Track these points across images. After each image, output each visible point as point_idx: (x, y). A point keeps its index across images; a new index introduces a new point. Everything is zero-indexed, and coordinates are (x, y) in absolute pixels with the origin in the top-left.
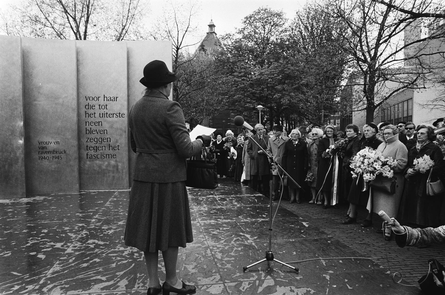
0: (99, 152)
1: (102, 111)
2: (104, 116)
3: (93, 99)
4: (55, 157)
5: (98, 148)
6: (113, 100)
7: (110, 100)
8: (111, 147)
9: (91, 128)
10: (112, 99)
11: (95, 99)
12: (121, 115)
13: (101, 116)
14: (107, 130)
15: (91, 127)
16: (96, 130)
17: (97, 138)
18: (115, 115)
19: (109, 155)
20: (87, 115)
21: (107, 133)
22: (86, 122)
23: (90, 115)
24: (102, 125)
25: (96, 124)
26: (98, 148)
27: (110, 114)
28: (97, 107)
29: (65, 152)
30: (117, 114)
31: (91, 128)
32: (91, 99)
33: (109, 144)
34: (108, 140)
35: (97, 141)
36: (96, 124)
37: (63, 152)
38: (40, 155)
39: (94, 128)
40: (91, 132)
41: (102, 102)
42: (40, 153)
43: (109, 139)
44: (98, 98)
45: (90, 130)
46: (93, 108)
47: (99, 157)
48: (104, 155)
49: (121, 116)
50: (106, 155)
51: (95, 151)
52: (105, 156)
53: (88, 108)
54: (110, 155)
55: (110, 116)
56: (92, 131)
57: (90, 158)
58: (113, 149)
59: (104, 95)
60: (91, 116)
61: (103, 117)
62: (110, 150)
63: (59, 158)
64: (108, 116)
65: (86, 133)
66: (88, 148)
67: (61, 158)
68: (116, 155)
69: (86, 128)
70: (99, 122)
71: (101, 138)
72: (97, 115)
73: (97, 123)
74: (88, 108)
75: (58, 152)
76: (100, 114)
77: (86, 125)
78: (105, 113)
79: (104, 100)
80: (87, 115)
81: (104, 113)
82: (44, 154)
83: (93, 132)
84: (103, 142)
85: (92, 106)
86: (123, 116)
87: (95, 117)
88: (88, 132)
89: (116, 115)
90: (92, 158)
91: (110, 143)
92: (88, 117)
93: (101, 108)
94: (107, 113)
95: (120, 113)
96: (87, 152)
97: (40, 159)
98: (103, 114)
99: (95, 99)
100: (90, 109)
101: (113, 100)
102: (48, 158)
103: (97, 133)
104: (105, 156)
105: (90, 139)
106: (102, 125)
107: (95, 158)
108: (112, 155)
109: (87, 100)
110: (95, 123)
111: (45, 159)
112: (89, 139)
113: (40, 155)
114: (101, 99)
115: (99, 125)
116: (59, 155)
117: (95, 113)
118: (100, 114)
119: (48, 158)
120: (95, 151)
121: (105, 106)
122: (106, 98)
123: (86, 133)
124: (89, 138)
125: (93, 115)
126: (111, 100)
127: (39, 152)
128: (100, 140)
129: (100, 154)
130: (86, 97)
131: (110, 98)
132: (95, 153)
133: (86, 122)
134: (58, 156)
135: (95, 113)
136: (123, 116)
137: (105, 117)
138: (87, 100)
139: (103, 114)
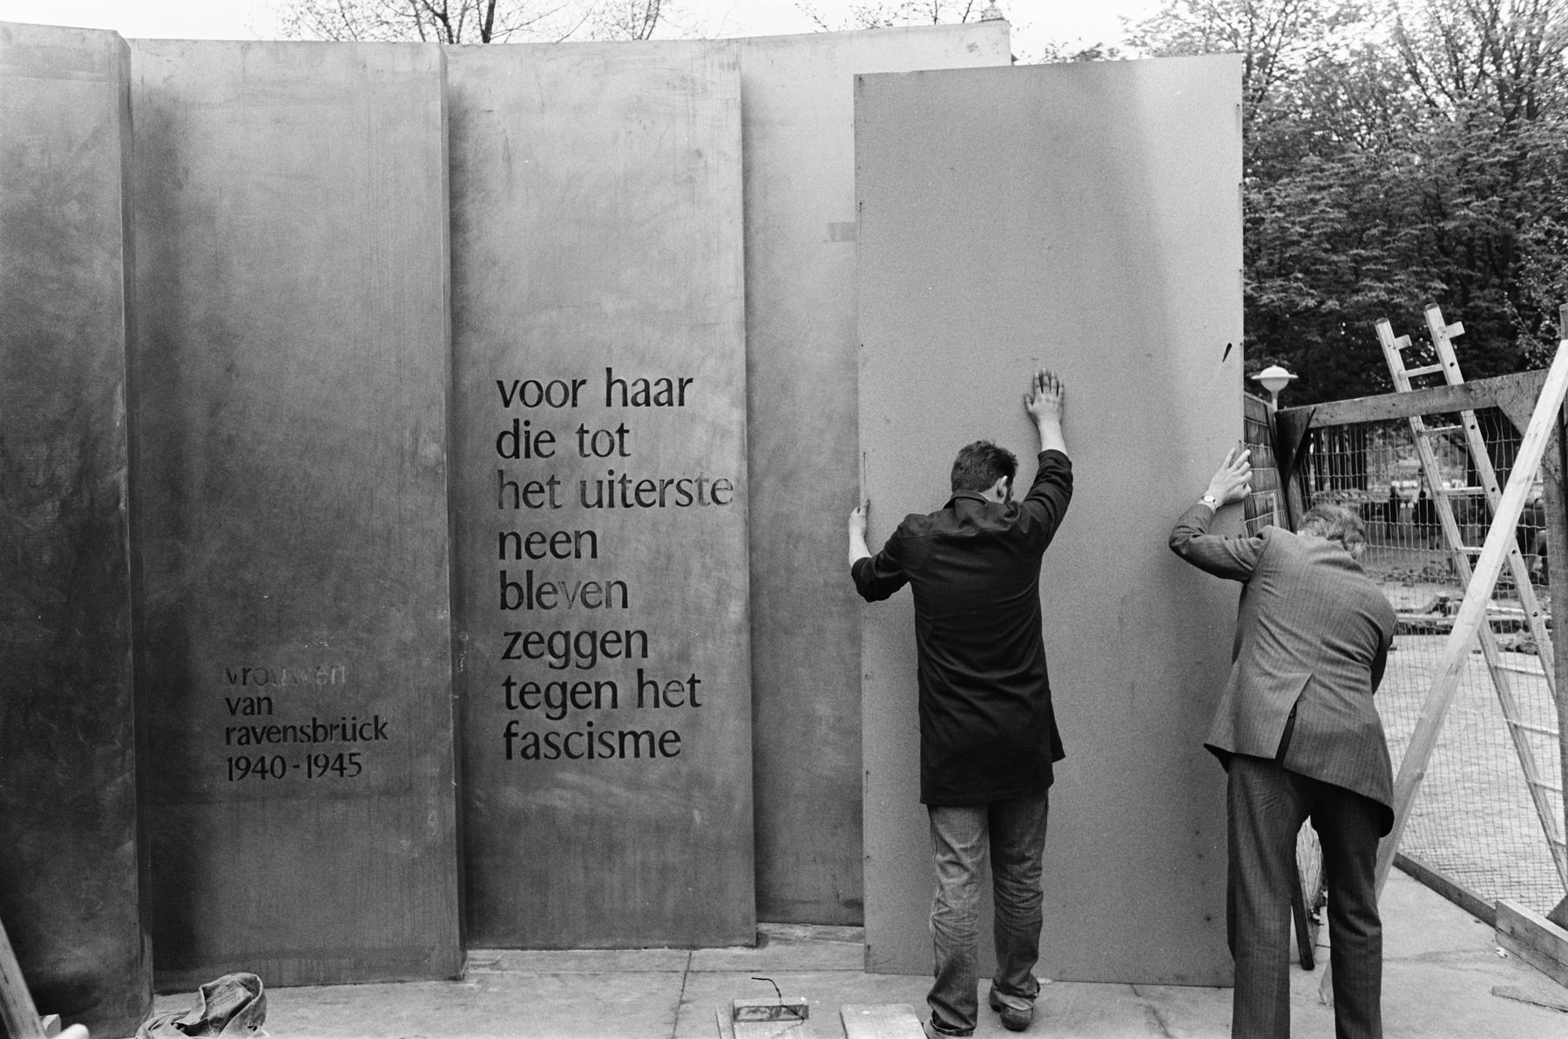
1: (596, 469)
2: (606, 501)
3: (544, 395)
5: (574, 692)
6: (663, 398)
7: (641, 398)
9: (530, 573)
10: (653, 391)
11: (557, 394)
13: (592, 498)
14: (622, 584)
18: (672, 489)
19: (637, 736)
20: (509, 490)
21: (625, 605)
22: (503, 538)
23: (523, 495)
24: (594, 555)
26: (574, 692)
29: (379, 732)
30: (684, 485)
31: (530, 573)
33: (640, 672)
34: (636, 641)
36: (560, 549)
38: (236, 750)
41: (593, 411)
42: (235, 737)
43: (636, 642)
46: (545, 448)
47: (575, 753)
49: (707, 497)
50: (622, 736)
53: (516, 454)
54: (644, 740)
57: (524, 753)
59: (609, 370)
60: (535, 499)
61: (599, 503)
62: (640, 705)
63: (342, 769)
64: (631, 498)
66: (515, 691)
67: (352, 770)
68: (678, 739)
69: (503, 573)
70: (579, 535)
71: (593, 636)
72: (567, 493)
73: (568, 540)
74: (516, 454)
76: (583, 483)
78: (617, 477)
79: (609, 404)
81: (606, 478)
82: (259, 741)
85: (537, 441)
89: (678, 485)
90: (537, 755)
91: (646, 664)
92: (517, 506)
93: (588, 449)
96: (508, 715)
97: (237, 773)
99: (557, 394)
100: (528, 455)
101: (663, 398)
102: (278, 769)
105: (526, 643)
106: (594, 555)
107: (552, 753)
108: (657, 740)
109: (507, 403)
111: (263, 772)
112: (520, 642)
113: (236, 750)
114: (594, 391)
115: (578, 555)
117: (552, 482)
119: (278, 769)
120: (558, 712)
121: (616, 437)
122: (617, 388)
123: (504, 605)
124: (518, 635)
125: (542, 490)
126: (647, 403)
127: (229, 732)
128: (586, 646)
129: (585, 730)
130: (500, 383)
131: (641, 386)
132: (556, 725)
133: (503, 538)
134: (341, 757)
135: (552, 482)
137: (611, 505)
138: (507, 403)
139: (600, 482)
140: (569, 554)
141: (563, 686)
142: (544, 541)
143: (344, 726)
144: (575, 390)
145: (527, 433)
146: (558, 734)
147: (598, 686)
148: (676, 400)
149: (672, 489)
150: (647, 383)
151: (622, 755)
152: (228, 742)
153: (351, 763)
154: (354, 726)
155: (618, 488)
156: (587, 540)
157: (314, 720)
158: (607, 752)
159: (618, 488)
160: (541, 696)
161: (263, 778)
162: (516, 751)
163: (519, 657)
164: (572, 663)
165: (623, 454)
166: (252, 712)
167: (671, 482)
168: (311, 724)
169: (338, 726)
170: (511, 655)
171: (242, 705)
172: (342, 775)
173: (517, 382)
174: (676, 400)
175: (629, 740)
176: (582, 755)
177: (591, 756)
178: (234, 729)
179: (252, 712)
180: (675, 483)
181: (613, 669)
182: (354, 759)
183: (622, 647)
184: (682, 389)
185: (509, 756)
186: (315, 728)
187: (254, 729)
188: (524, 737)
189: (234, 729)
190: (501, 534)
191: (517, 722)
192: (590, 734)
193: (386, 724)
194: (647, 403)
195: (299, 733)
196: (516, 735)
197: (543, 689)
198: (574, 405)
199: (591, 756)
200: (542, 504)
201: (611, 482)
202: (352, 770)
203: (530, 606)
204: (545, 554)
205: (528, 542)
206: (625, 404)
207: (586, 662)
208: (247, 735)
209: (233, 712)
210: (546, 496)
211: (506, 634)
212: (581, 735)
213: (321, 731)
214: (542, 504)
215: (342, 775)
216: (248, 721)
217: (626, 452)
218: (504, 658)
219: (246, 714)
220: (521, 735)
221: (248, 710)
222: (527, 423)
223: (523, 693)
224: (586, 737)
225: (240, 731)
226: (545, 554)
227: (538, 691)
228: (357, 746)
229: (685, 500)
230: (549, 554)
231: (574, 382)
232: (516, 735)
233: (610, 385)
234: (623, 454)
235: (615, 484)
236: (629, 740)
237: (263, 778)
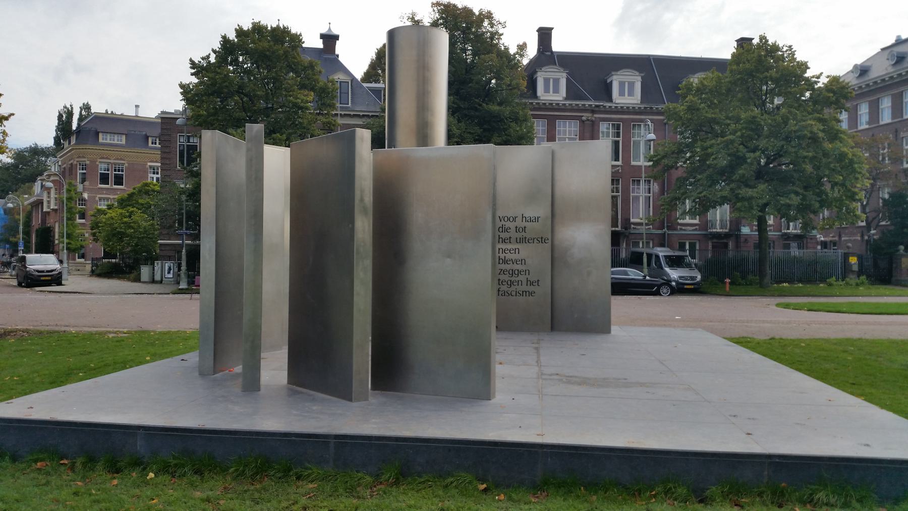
0: (513, 288)
1: (519, 235)
2: (521, 242)
3: (509, 219)
6: (534, 221)
7: (529, 221)
10: (532, 219)
12: (543, 240)
13: (518, 241)
15: (504, 254)
17: (512, 270)
18: (535, 240)
19: (526, 292)
22: (499, 249)
25: (512, 252)
28: (513, 229)
30: (538, 239)
32: (506, 219)
33: (527, 278)
36: (512, 252)
39: (509, 256)
40: (505, 261)
41: (519, 223)
44: (514, 219)
45: (504, 259)
50: (523, 292)
51: (509, 286)
54: (528, 293)
57: (502, 295)
58: (532, 284)
59: (523, 215)
62: (527, 285)
64: (527, 241)
66: (500, 282)
69: (499, 257)
71: (518, 270)
76: (517, 238)
78: (524, 237)
80: (501, 239)
81: (522, 237)
84: (519, 274)
85: (507, 229)
90: (504, 295)
94: (525, 238)
95: (542, 238)
98: (520, 238)
101: (534, 221)
105: (504, 271)
107: (508, 295)
109: (501, 221)
112: (502, 271)
114: (519, 219)
118: (517, 238)
123: (499, 263)
124: (502, 270)
128: (516, 272)
132: (509, 289)
135: (510, 238)
136: (546, 241)
137: (523, 243)
138: (501, 221)
139: (520, 238)
144: (515, 218)
148: (537, 221)
149: (535, 240)
151: (523, 295)
156: (517, 250)
158: (519, 295)
162: (500, 294)
174: (537, 221)
175: (524, 293)
181: (521, 278)
183: (524, 273)
185: (499, 295)
203: (505, 264)
233: (523, 217)
236: (524, 293)
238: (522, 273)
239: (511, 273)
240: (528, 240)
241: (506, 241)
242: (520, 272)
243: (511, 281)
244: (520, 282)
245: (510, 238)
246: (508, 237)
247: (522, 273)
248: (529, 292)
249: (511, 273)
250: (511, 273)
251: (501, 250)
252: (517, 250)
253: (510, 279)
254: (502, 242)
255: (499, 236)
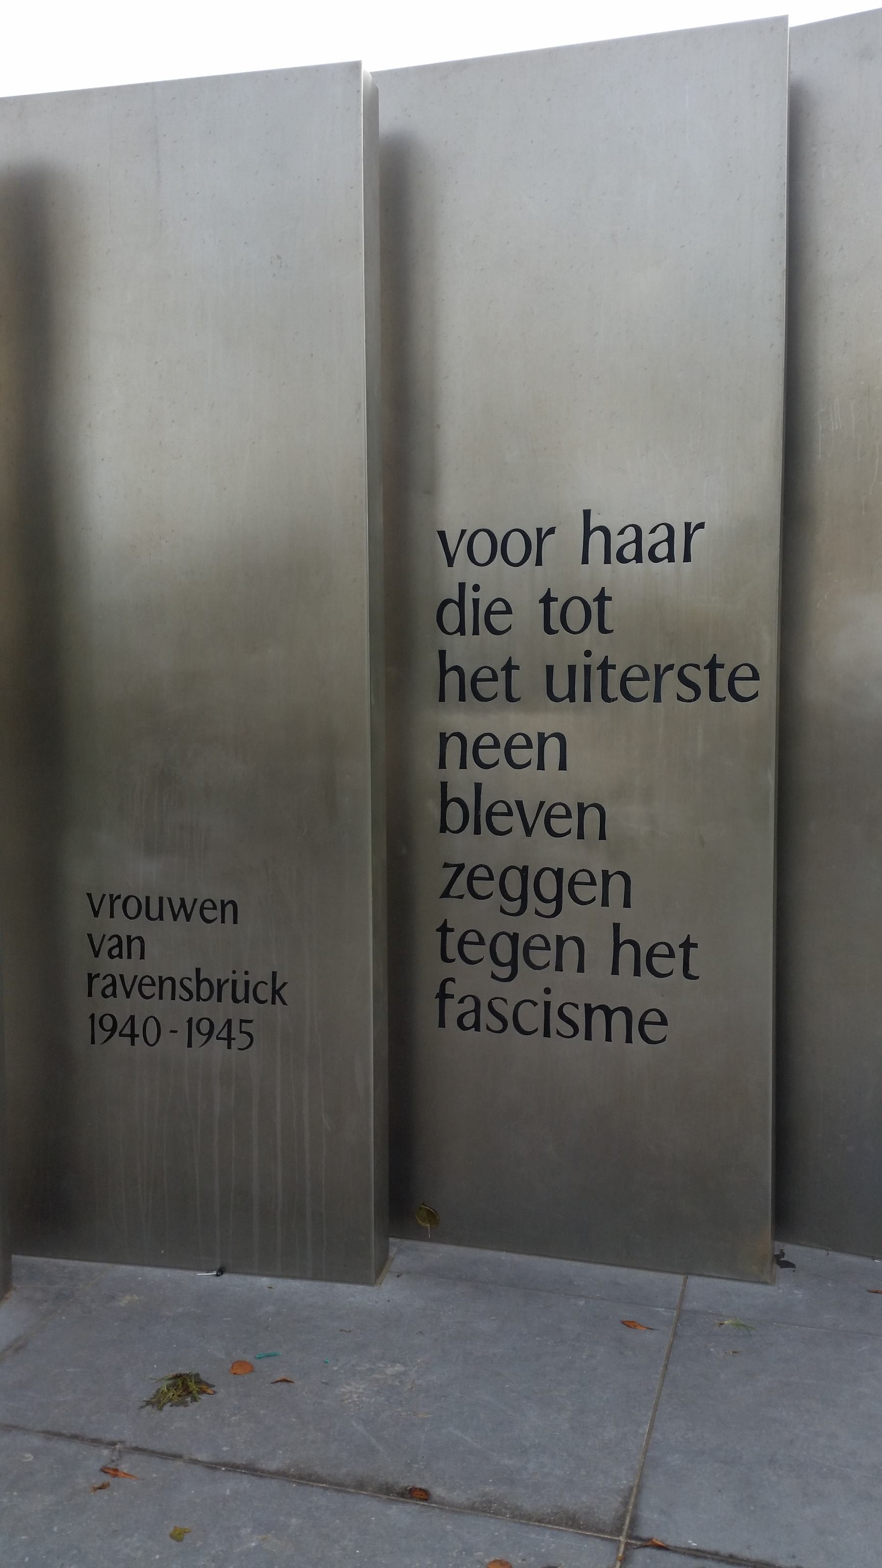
4: (205, 1027)
6: (662, 551)
8: (627, 951)
9: (478, 787)
10: (647, 542)
12: (722, 677)
15: (474, 772)
16: (520, 804)
18: (670, 679)
19: (609, 1013)
22: (444, 739)
24: (563, 766)
26: (527, 947)
27: (636, 673)
30: (689, 673)
31: (478, 787)
33: (616, 927)
35: (524, 897)
37: (265, 992)
46: (498, 621)
48: (568, 1011)
51: (506, 972)
52: (578, 1017)
53: (461, 630)
55: (635, 688)
56: (490, 814)
59: (587, 514)
61: (571, 697)
63: (229, 1039)
64: (614, 690)
65: (444, 828)
66: (452, 940)
69: (444, 785)
71: (559, 874)
74: (461, 630)
75: (227, 989)
76: (550, 670)
77: (442, 765)
78: (596, 660)
80: (452, 678)
81: (581, 662)
83: (500, 823)
85: (489, 612)
86: (739, 686)
87: (510, 698)
88: (455, 814)
89: (682, 678)
90: (477, 1026)
93: (555, 623)
94: (605, 666)
95: (713, 666)
96: (447, 970)
97: (101, 1035)
98: (572, 669)
100: (476, 632)
101: (662, 551)
102: (152, 1036)
103: (529, 831)
104: (578, 1017)
105: (471, 878)
106: (563, 766)
107: (498, 1025)
110: (509, 747)
111: (133, 1036)
115: (541, 766)
116: (235, 1012)
118: (550, 670)
119: (152, 1036)
121: (594, 607)
122: (598, 538)
123: (444, 828)
125: (495, 678)
126: (638, 558)
128: (549, 887)
129: (541, 998)
130: (442, 535)
131: (631, 534)
133: (444, 739)
134: (229, 1022)
135: (509, 667)
137: (587, 698)
138: (450, 561)
139: (572, 669)
140: (529, 763)
141: (514, 938)
142: (497, 745)
143: (234, 982)
145: (476, 602)
146: (505, 1001)
147: (560, 941)
150: (638, 530)
151: (588, 1037)
152: (90, 995)
153: (241, 1032)
154: (247, 983)
155: (596, 676)
156: (552, 746)
157: (198, 971)
159: (596, 676)
160: (486, 948)
161: (133, 1043)
163: (461, 897)
164: (530, 909)
165: (602, 629)
166: (120, 956)
167: (670, 667)
168: (193, 976)
169: (227, 981)
170: (451, 893)
171: (108, 945)
172: (229, 1047)
173: (463, 532)
176: (536, 1030)
177: (547, 1034)
178: (98, 975)
179: (120, 956)
180: (676, 669)
182: (246, 1027)
184: (688, 538)
185: (442, 1024)
186: (199, 982)
187: (122, 976)
188: (462, 1001)
189: (98, 975)
190: (442, 735)
191: (453, 980)
192: (547, 1005)
193: (284, 984)
194: (638, 558)
195: (179, 990)
196: (452, 996)
197: (488, 941)
198: (539, 562)
199: (547, 1034)
200: (496, 695)
201: (587, 668)
202: (241, 1040)
203: (477, 831)
204: (497, 763)
205: (477, 746)
206: (607, 560)
207: (552, 907)
208: (114, 984)
209: (97, 954)
210: (500, 686)
211: (446, 865)
212: (535, 1004)
213: (205, 988)
214: (496, 695)
215: (229, 1047)
216: (117, 966)
217: (607, 626)
218: (442, 897)
219: (112, 957)
220: (457, 998)
221: (115, 952)
222: (476, 588)
223: (462, 942)
224: (541, 1007)
225: (104, 978)
226: (497, 763)
227: (481, 942)
228: (251, 1009)
229: (689, 693)
230: (503, 761)
231: (539, 531)
232: (452, 996)
234: (602, 629)
235: (593, 669)
237: (133, 1043)
238: (583, 893)
239: (514, 889)
240: (625, 679)
241: (484, 688)
242: (572, 882)
243: (514, 938)
244: (571, 950)
245: (509, 667)
246: (498, 666)
247: (583, 893)
248: (627, 1011)
249: (514, 885)
250: (514, 885)
251: (454, 747)
252: (552, 746)
253: (512, 925)
254: (462, 698)
255: (442, 654)
